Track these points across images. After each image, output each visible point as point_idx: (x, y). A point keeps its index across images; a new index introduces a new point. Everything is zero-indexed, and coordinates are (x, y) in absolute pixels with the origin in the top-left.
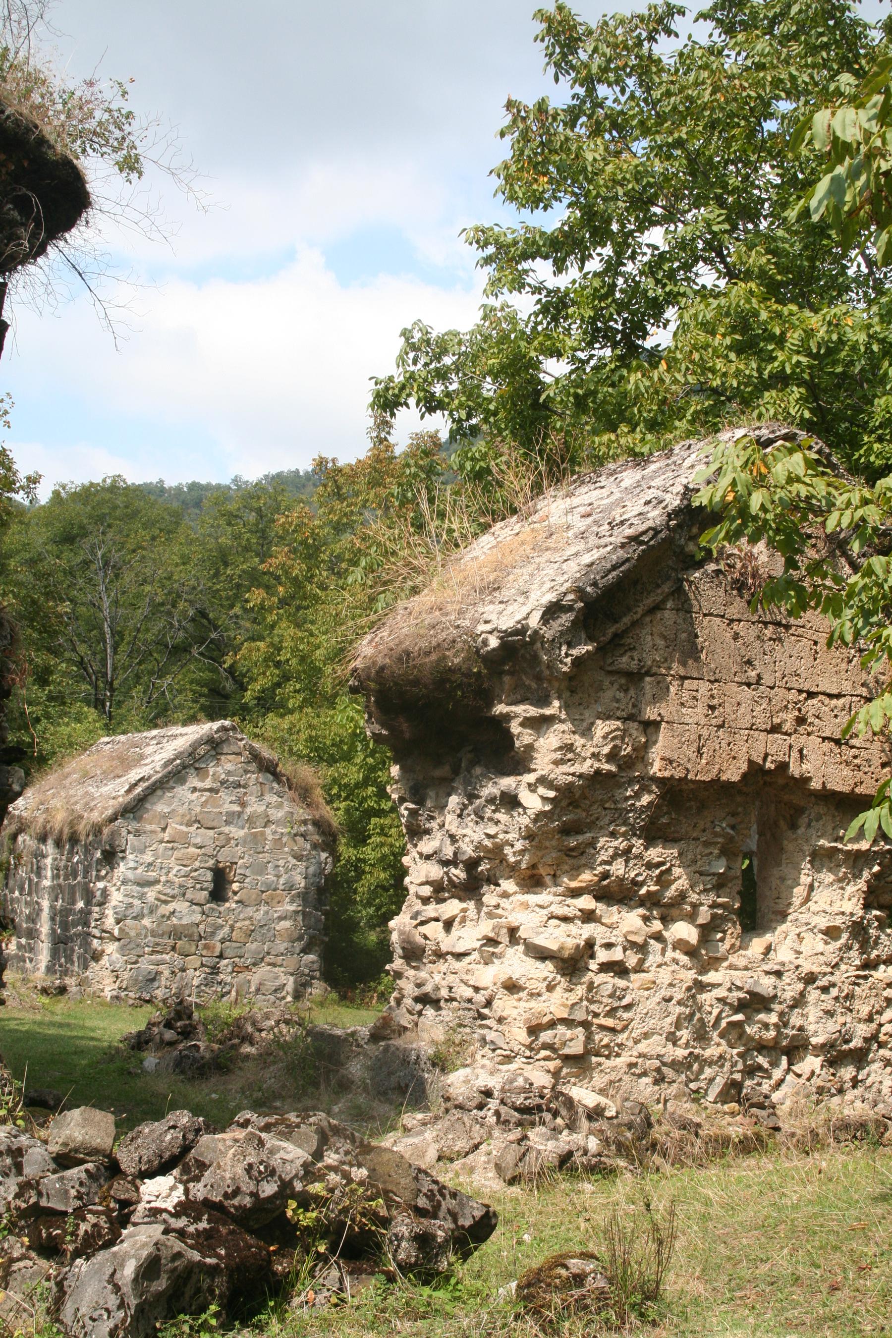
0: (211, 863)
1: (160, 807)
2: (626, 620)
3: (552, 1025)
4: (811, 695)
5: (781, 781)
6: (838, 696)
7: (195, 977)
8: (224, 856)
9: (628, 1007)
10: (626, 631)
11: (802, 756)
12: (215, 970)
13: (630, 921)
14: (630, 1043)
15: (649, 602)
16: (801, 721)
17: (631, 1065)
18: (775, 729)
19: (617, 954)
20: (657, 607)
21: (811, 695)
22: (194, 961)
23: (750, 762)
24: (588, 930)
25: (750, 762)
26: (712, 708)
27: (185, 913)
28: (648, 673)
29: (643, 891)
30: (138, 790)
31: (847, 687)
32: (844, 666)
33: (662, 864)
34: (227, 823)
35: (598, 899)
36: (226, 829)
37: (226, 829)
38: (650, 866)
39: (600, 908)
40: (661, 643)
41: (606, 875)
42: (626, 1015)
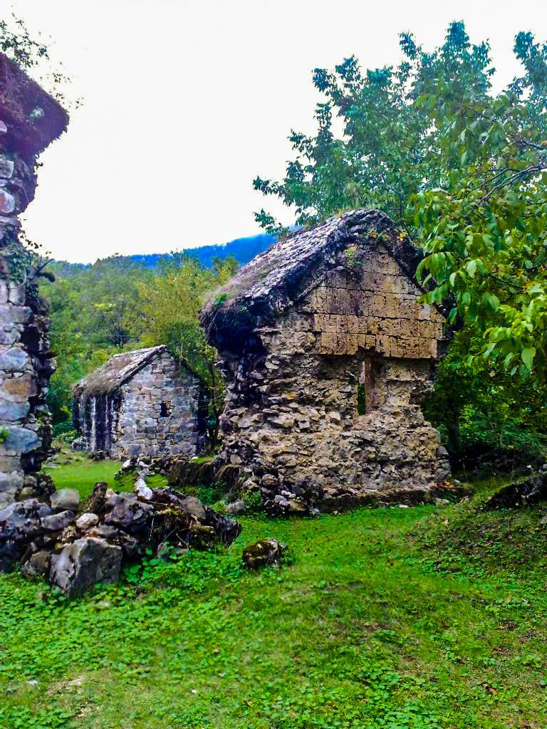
0: (160, 402)
1: (137, 379)
2: (305, 291)
3: (283, 453)
4: (383, 319)
5: (372, 354)
6: (396, 318)
7: (155, 447)
8: (165, 398)
9: (313, 446)
10: (306, 295)
11: (381, 344)
12: (164, 444)
13: (313, 411)
14: (314, 461)
15: (313, 284)
16: (380, 329)
17: (315, 470)
18: (369, 333)
19: (307, 425)
20: (318, 286)
21: (383, 319)
22: (155, 441)
23: (359, 347)
24: (297, 416)
25: (359, 347)
26: (342, 326)
27: (151, 422)
28: (316, 313)
29: (317, 400)
30: (129, 374)
31: (399, 315)
32: (397, 306)
33: (323, 389)
34: (166, 385)
35: (299, 403)
36: (165, 388)
37: (165, 388)
38: (320, 390)
39: (300, 408)
40: (320, 300)
41: (302, 394)
42: (312, 450)
